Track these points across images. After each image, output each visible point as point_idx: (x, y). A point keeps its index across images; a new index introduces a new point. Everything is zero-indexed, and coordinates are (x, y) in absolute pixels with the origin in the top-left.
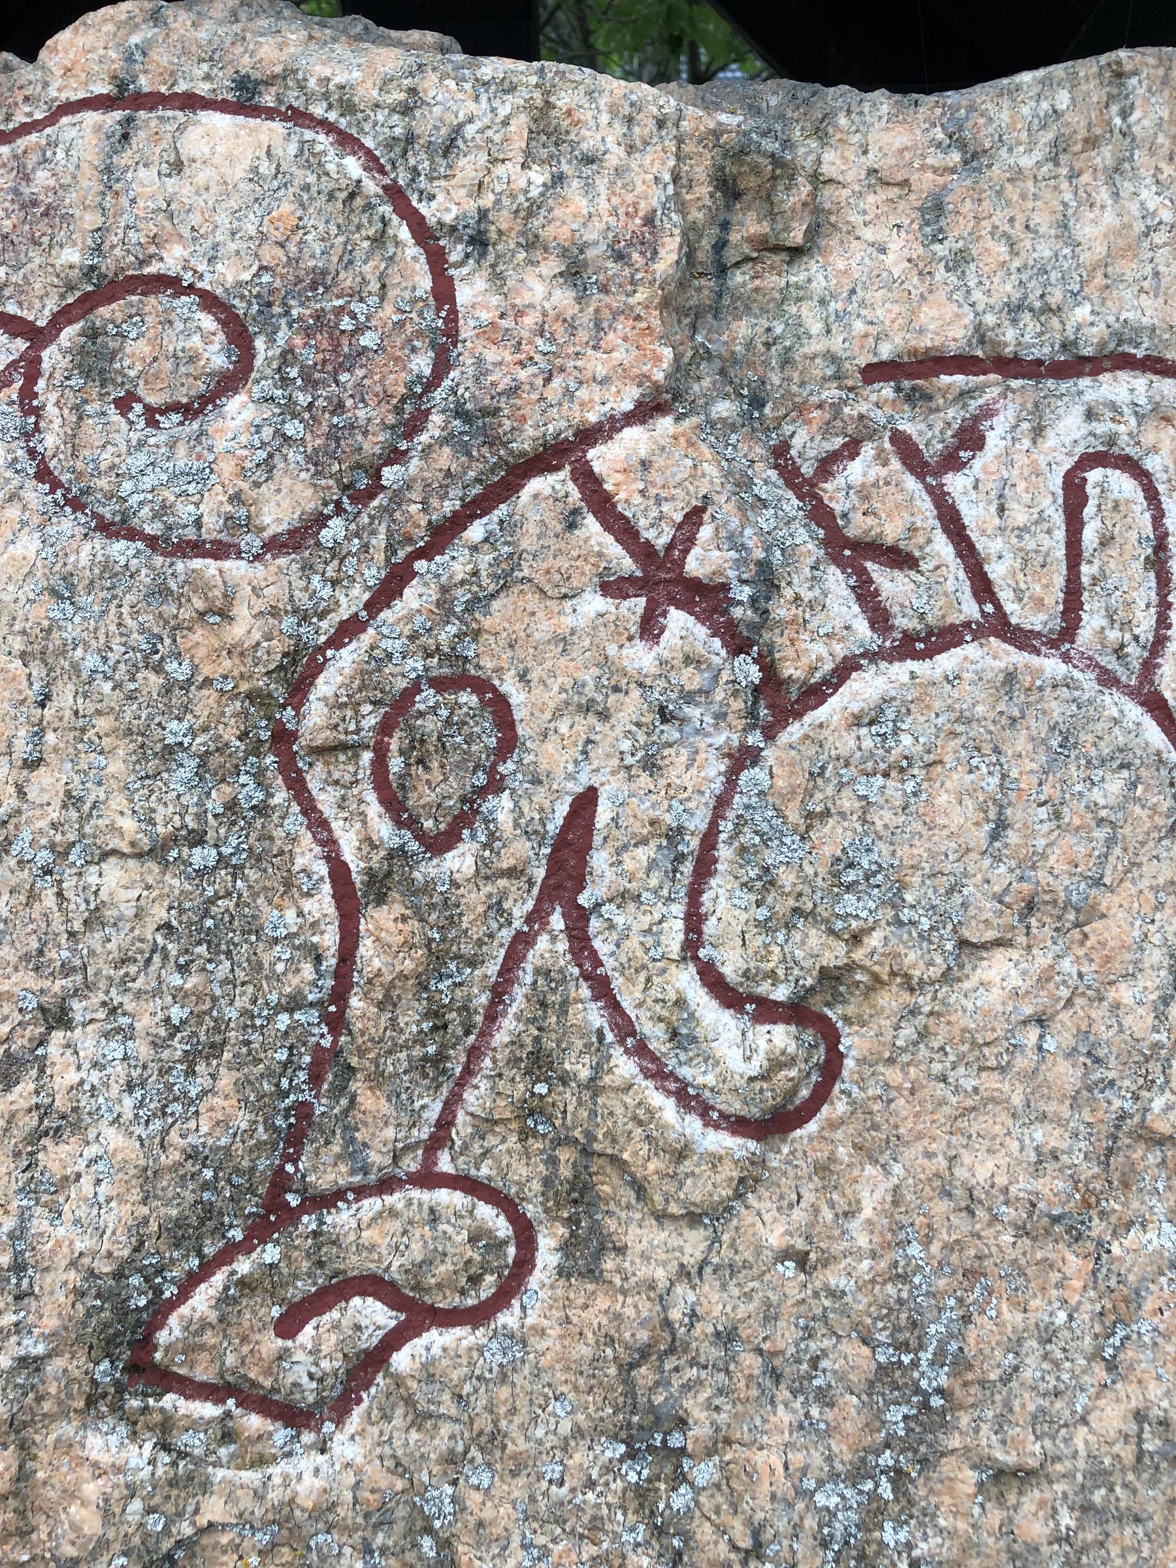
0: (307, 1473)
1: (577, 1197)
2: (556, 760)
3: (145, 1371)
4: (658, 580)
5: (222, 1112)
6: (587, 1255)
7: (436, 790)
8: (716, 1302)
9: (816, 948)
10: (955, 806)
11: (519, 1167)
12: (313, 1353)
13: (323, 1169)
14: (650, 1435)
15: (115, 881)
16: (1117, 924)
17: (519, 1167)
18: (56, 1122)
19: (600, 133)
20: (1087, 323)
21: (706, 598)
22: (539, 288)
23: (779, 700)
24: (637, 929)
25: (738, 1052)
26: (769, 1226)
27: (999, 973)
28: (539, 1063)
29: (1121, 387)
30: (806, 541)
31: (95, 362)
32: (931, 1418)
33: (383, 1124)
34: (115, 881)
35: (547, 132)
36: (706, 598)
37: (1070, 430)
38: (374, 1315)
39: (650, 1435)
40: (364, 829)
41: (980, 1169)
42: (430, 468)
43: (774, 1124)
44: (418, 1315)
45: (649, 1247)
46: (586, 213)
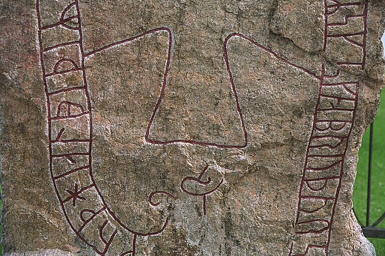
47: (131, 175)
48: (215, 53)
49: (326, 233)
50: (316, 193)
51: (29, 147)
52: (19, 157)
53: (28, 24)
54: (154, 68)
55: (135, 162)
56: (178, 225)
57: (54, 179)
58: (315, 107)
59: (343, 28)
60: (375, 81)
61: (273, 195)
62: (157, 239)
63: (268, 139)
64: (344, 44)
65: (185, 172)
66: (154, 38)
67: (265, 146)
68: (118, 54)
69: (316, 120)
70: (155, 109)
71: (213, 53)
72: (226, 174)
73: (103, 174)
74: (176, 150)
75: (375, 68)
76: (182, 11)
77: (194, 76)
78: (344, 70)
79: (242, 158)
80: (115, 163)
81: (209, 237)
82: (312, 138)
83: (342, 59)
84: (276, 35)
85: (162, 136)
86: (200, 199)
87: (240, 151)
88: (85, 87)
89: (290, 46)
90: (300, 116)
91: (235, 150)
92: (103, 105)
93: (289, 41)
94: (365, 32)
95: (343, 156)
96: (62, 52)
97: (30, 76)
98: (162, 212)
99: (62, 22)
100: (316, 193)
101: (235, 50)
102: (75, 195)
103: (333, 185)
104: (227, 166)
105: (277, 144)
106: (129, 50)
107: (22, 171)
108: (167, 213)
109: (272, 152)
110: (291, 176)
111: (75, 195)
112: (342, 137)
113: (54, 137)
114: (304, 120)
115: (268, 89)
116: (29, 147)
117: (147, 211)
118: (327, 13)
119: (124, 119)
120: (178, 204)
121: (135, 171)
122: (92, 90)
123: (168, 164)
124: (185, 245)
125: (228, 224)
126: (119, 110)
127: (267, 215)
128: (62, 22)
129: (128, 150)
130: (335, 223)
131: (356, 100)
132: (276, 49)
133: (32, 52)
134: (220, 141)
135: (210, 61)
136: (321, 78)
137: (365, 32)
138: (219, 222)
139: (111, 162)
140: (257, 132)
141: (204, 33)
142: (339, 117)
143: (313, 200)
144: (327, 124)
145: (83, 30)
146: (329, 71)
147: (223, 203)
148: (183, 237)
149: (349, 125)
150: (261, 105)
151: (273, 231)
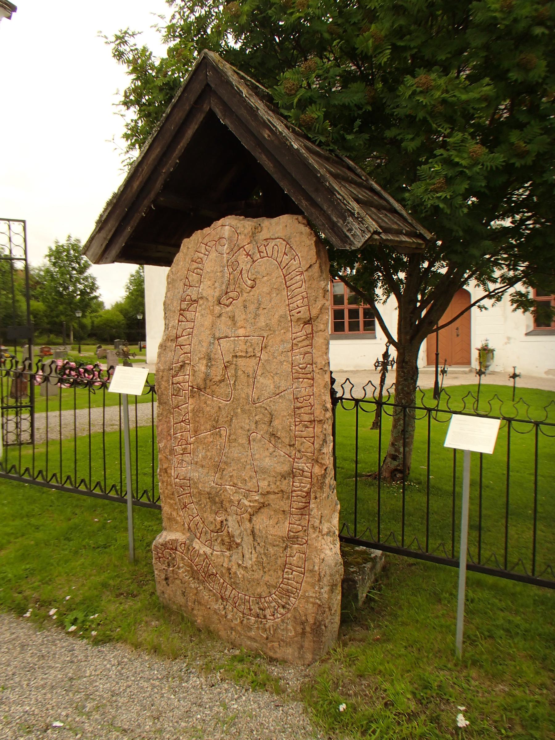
0: (228, 309)
1: (241, 291)
2: (241, 266)
4: (248, 255)
5: (224, 287)
6: (242, 295)
7: (234, 268)
8: (249, 298)
9: (254, 276)
10: (263, 268)
11: (238, 290)
12: (228, 302)
13: (229, 291)
15: (218, 274)
16: (273, 275)
18: (215, 288)
19: (247, 226)
20: (276, 236)
21: (250, 255)
22: (243, 237)
23: (254, 262)
24: (245, 276)
25: (249, 282)
26: (251, 293)
27: (265, 278)
29: (278, 240)
30: (257, 252)
31: (219, 243)
32: (260, 304)
33: (232, 287)
34: (218, 274)
35: (244, 226)
36: (250, 255)
37: (273, 244)
38: (231, 300)
39: (245, 307)
40: (231, 270)
41: (264, 290)
42: (236, 249)
43: (252, 287)
45: (245, 295)
46: (246, 231)
47: (208, 500)
48: (244, 441)
49: (305, 546)
50: (298, 522)
52: (165, 484)
53: (169, 422)
54: (218, 447)
55: (209, 493)
56: (230, 530)
58: (292, 474)
59: (304, 434)
60: (321, 463)
61: (276, 520)
62: (222, 536)
63: (269, 489)
64: (304, 442)
65: (231, 501)
66: (219, 432)
67: (268, 493)
68: (205, 438)
69: (293, 482)
70: (218, 468)
71: (244, 441)
72: (250, 506)
73: (196, 498)
74: (225, 490)
75: (320, 457)
76: (231, 419)
77: (235, 452)
78: (305, 455)
79: (257, 498)
80: (200, 493)
81: (245, 538)
82: (292, 491)
83: (303, 450)
84: (273, 435)
85: (220, 481)
86: (239, 517)
87: (256, 494)
90: (285, 479)
91: (254, 493)
92: (196, 463)
93: (279, 438)
94: (314, 437)
95: (309, 503)
96: (182, 435)
97: (168, 446)
98: (222, 522)
99: (182, 421)
100: (298, 522)
101: (254, 440)
102: (186, 506)
103: (305, 519)
104: (250, 501)
105: (275, 493)
106: (209, 436)
107: (166, 491)
108: (225, 523)
109: (272, 496)
110: (284, 511)
112: (307, 493)
114: (287, 481)
115: (267, 462)
117: (215, 520)
118: (296, 425)
119: (206, 471)
120: (230, 518)
121: (209, 498)
123: (223, 497)
124: (234, 541)
125: (253, 532)
126: (202, 466)
127: (272, 531)
128: (182, 421)
129: (205, 487)
130: (309, 542)
131: (311, 473)
132: (273, 442)
134: (247, 488)
135: (242, 445)
136: (294, 459)
137: (314, 437)
138: (249, 531)
139: (199, 493)
140: (263, 484)
141: (240, 431)
142: (304, 481)
143: (295, 526)
144: (298, 484)
146: (298, 455)
147: (250, 521)
148: (233, 537)
149: (309, 486)
150: (264, 471)
151: (276, 541)
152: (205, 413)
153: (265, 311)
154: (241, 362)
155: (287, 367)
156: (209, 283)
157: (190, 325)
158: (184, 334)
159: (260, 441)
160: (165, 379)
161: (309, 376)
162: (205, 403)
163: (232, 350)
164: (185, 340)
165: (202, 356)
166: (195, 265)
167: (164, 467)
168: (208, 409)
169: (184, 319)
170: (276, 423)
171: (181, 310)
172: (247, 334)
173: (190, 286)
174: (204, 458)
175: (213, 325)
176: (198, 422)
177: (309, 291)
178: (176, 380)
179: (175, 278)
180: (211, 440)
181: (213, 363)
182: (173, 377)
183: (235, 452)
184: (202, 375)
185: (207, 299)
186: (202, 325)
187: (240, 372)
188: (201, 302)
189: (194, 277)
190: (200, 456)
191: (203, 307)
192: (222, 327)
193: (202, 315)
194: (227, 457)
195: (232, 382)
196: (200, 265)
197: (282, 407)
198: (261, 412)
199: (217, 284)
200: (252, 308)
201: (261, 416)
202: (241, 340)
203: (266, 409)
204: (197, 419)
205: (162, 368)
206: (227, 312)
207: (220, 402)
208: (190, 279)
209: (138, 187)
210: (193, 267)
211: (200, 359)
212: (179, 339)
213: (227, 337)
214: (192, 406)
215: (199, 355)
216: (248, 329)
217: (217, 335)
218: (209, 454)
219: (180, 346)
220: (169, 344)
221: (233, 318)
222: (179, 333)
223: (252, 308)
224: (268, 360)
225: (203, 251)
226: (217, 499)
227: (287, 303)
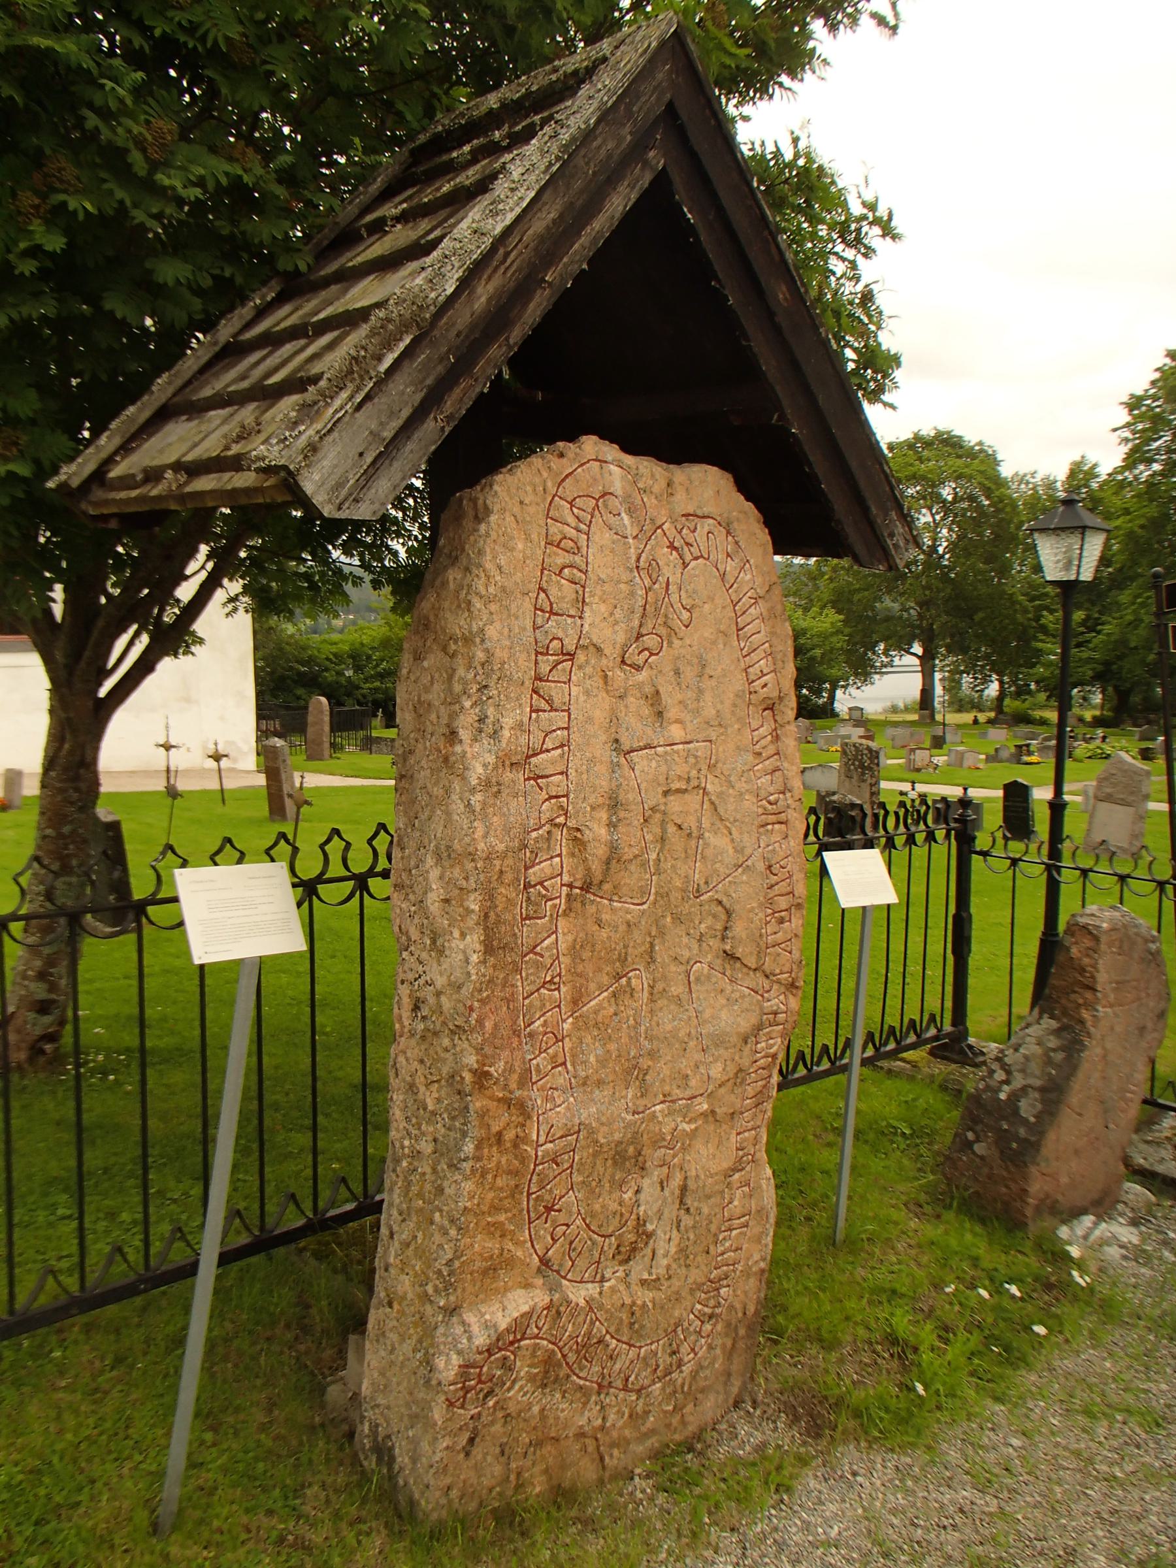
3: (623, 662)
6: (670, 643)
13: (644, 631)
14: (677, 673)
17: (663, 631)
18: (616, 623)
28: (666, 616)
34: (622, 586)
37: (706, 529)
39: (677, 673)
40: (647, 582)
44: (651, 654)
51: (504, 1160)
52: (489, 1177)
57: (529, 1194)
70: (635, 1073)
76: (652, 945)
77: (667, 1020)
78: (779, 982)
84: (730, 956)
88: (564, 1064)
89: (738, 965)
96: (545, 1024)
106: (606, 1004)
111: (549, 1209)
113: (542, 1139)
116: (504, 1160)
122: (573, 1065)
133: (516, 1033)
134: (688, 1093)
145: (563, 989)
152: (598, 947)
153: (713, 682)
154: (675, 805)
155: (749, 804)
156: (603, 608)
157: (560, 719)
158: (549, 744)
159: (708, 977)
160: (508, 877)
161: (783, 817)
162: (599, 923)
163: (662, 779)
164: (553, 762)
165: (601, 800)
166: (561, 558)
167: (495, 1129)
168: (604, 934)
169: (543, 705)
170: (739, 929)
171: (538, 678)
172: (689, 738)
173: (551, 612)
174: (602, 1062)
175: (614, 719)
176: (580, 975)
177: (775, 641)
178: (534, 874)
179: (509, 584)
180: (612, 1010)
181: (622, 814)
182: (526, 868)
183: (667, 1020)
184: (601, 851)
185: (599, 649)
186: (590, 720)
187: (671, 829)
188: (581, 657)
189: (562, 591)
190: (592, 1059)
191: (589, 670)
192: (632, 720)
193: (587, 693)
194: (651, 1040)
195: (653, 856)
196: (577, 558)
197: (745, 892)
198: (709, 913)
199: (618, 614)
200: (689, 673)
201: (710, 921)
202: (677, 752)
203: (720, 903)
204: (580, 968)
205: (501, 847)
206: (640, 686)
207: (628, 912)
208: (553, 592)
209: (489, 300)
210: (560, 561)
211: (593, 808)
212: (533, 760)
213: (648, 746)
214: (570, 938)
215: (592, 800)
216: (689, 726)
217: (626, 745)
218: (612, 1047)
219: (537, 778)
220: (508, 775)
221: (654, 698)
222: (536, 739)
223: (689, 673)
224: (722, 793)
225: (571, 520)
226: (631, 1150)
227: (743, 666)
